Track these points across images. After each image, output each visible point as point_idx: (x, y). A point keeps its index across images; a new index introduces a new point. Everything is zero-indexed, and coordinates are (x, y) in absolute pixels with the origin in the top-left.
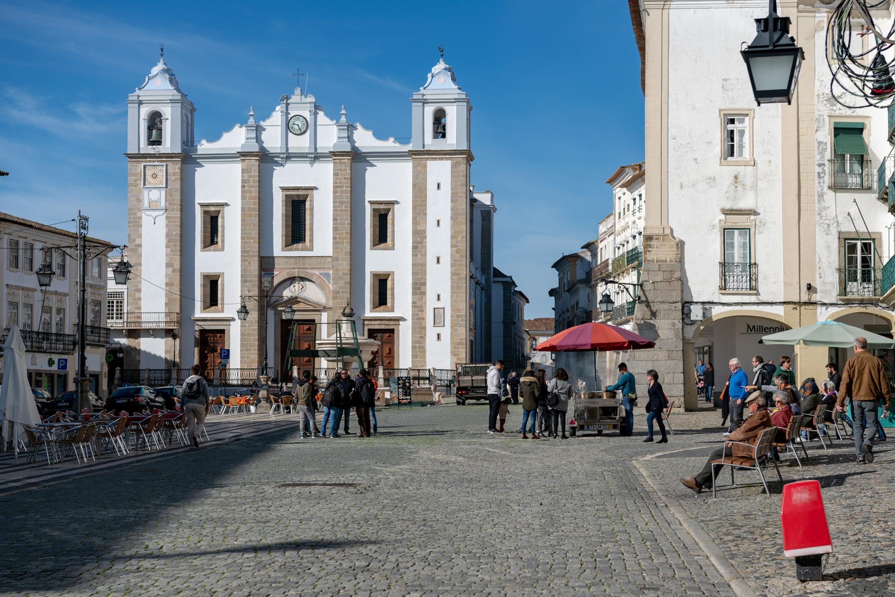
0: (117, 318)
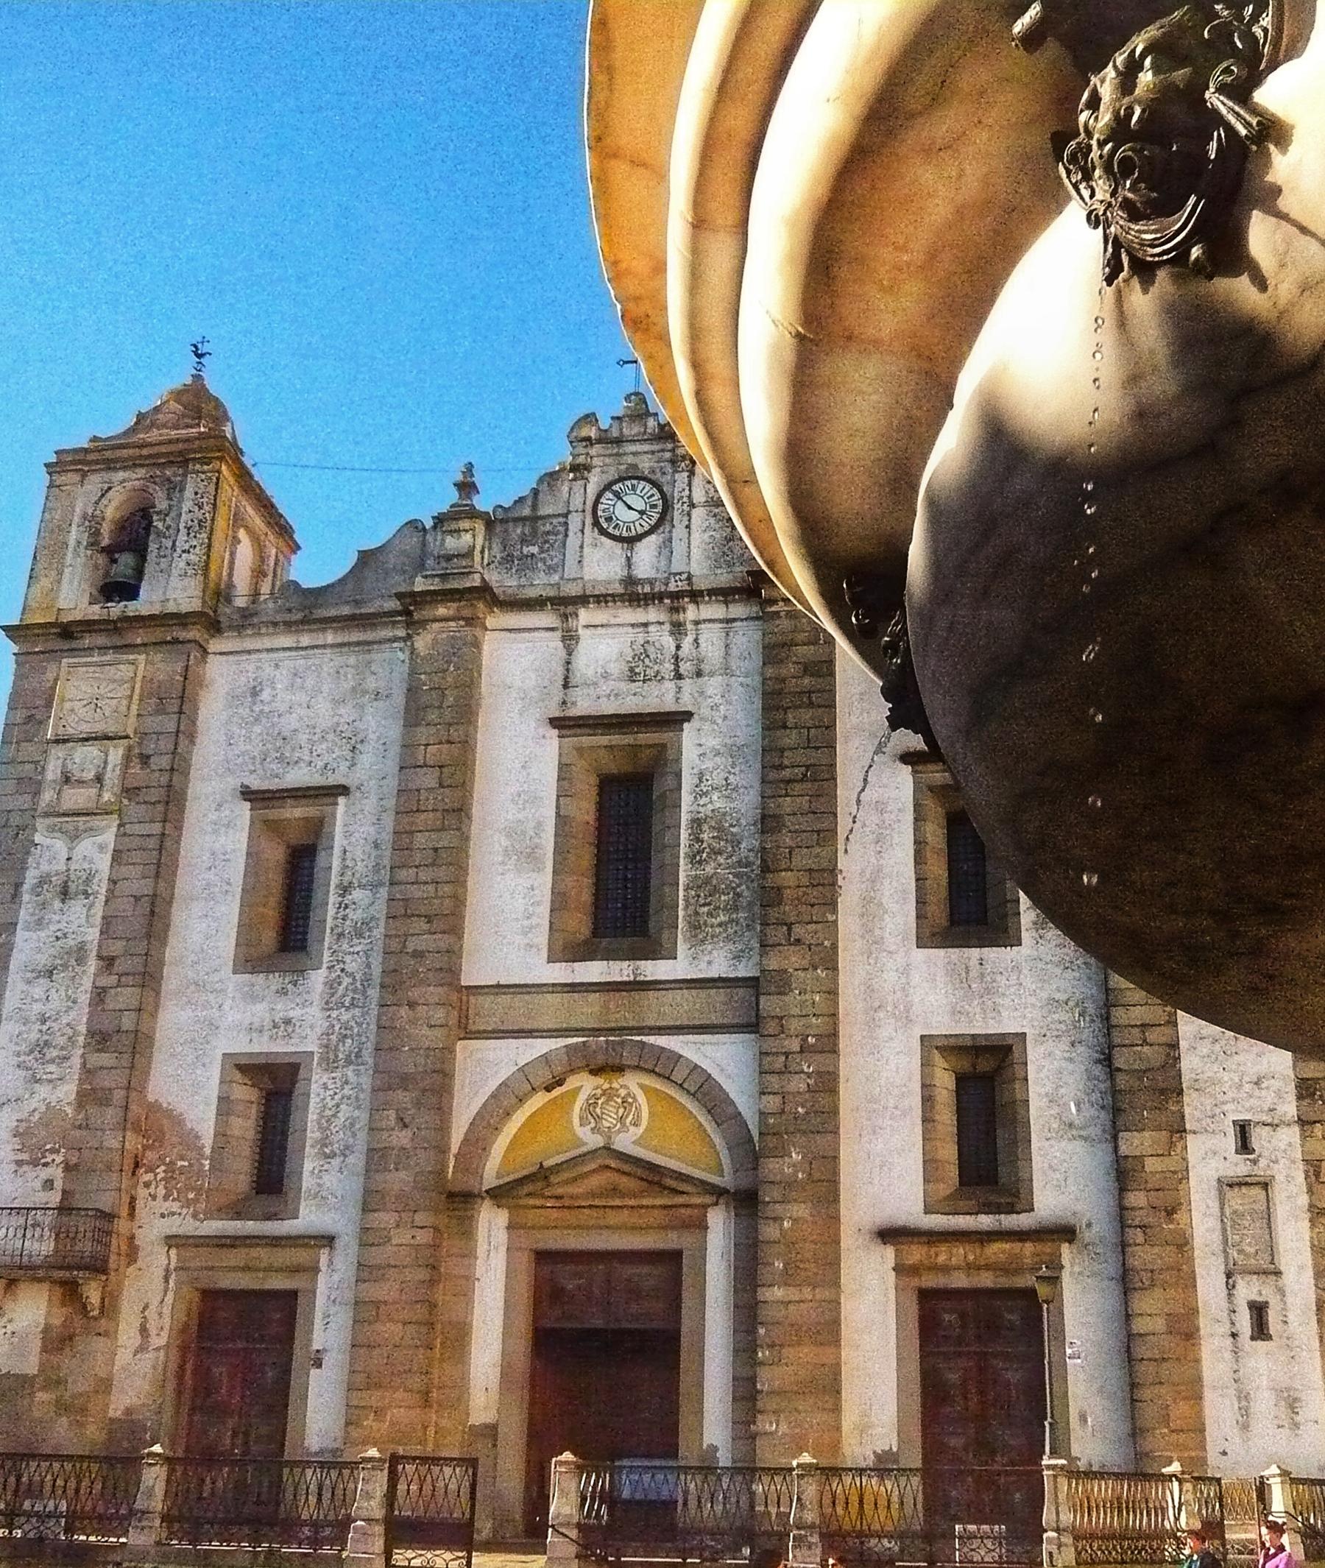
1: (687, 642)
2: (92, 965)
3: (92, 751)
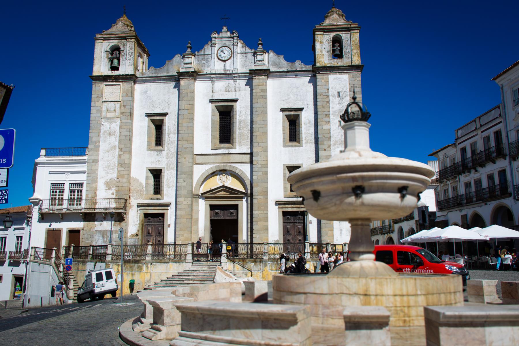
0: (77, 205)
1: (237, 83)
2: (117, 150)
3: (112, 104)
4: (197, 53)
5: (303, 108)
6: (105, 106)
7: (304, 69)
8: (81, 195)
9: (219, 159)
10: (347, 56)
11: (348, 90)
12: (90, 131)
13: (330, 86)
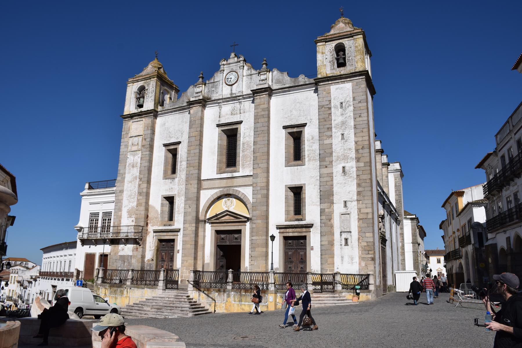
3: (136, 138)
4: (207, 82)
5: (306, 124)
6: (131, 141)
7: (307, 83)
8: (110, 223)
9: (224, 183)
10: (351, 63)
11: (352, 99)
12: (119, 164)
13: (332, 97)
